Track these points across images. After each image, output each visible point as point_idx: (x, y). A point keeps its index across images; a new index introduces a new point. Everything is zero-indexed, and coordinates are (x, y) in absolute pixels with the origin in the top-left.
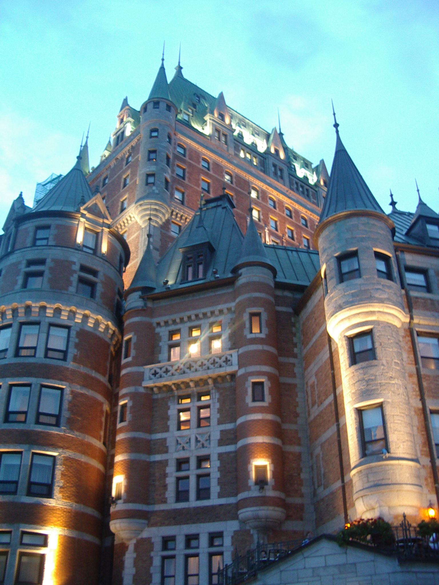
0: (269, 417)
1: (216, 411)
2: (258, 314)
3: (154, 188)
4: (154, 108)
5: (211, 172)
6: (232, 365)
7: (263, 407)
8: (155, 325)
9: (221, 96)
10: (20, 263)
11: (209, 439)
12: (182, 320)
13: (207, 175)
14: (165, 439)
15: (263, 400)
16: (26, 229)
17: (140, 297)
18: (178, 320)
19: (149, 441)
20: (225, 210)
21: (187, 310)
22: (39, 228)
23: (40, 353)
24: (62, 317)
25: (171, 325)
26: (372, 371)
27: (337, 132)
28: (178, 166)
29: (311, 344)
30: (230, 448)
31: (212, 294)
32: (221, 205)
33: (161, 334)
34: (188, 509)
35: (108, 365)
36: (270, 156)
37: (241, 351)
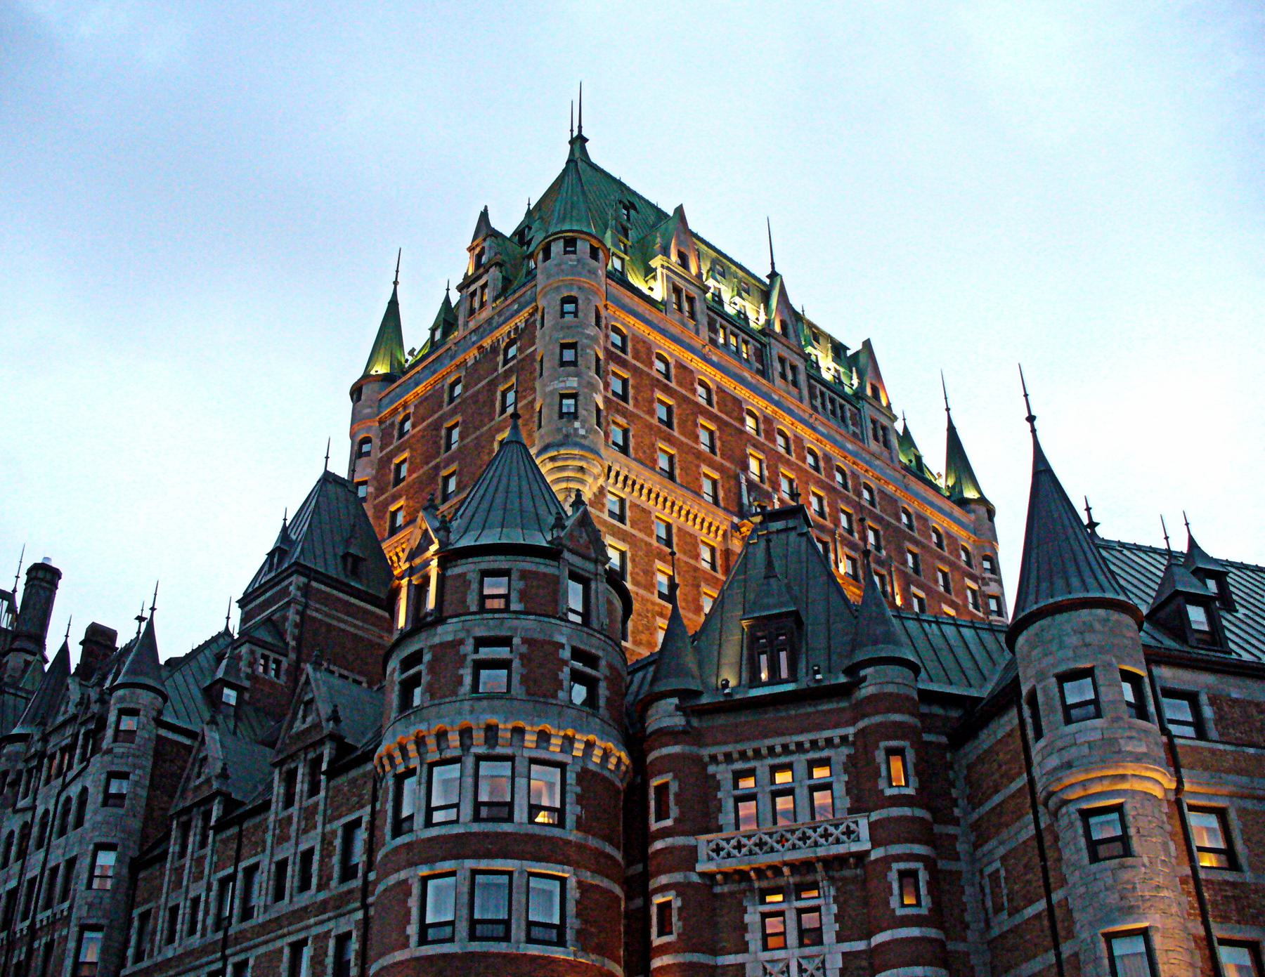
0: (932, 933)
1: (833, 917)
3: (577, 424)
4: (566, 252)
5: (673, 385)
6: (859, 840)
7: (918, 916)
8: (707, 759)
9: (680, 211)
12: (757, 752)
13: (667, 390)
16: (463, 575)
17: (678, 708)
20: (804, 539)
21: (766, 736)
22: (486, 573)
24: (552, 748)
25: (737, 761)
26: (1125, 875)
27: (1033, 431)
28: (615, 374)
29: (988, 806)
31: (810, 710)
32: (794, 528)
33: (719, 777)
36: (773, 341)
37: (875, 816)
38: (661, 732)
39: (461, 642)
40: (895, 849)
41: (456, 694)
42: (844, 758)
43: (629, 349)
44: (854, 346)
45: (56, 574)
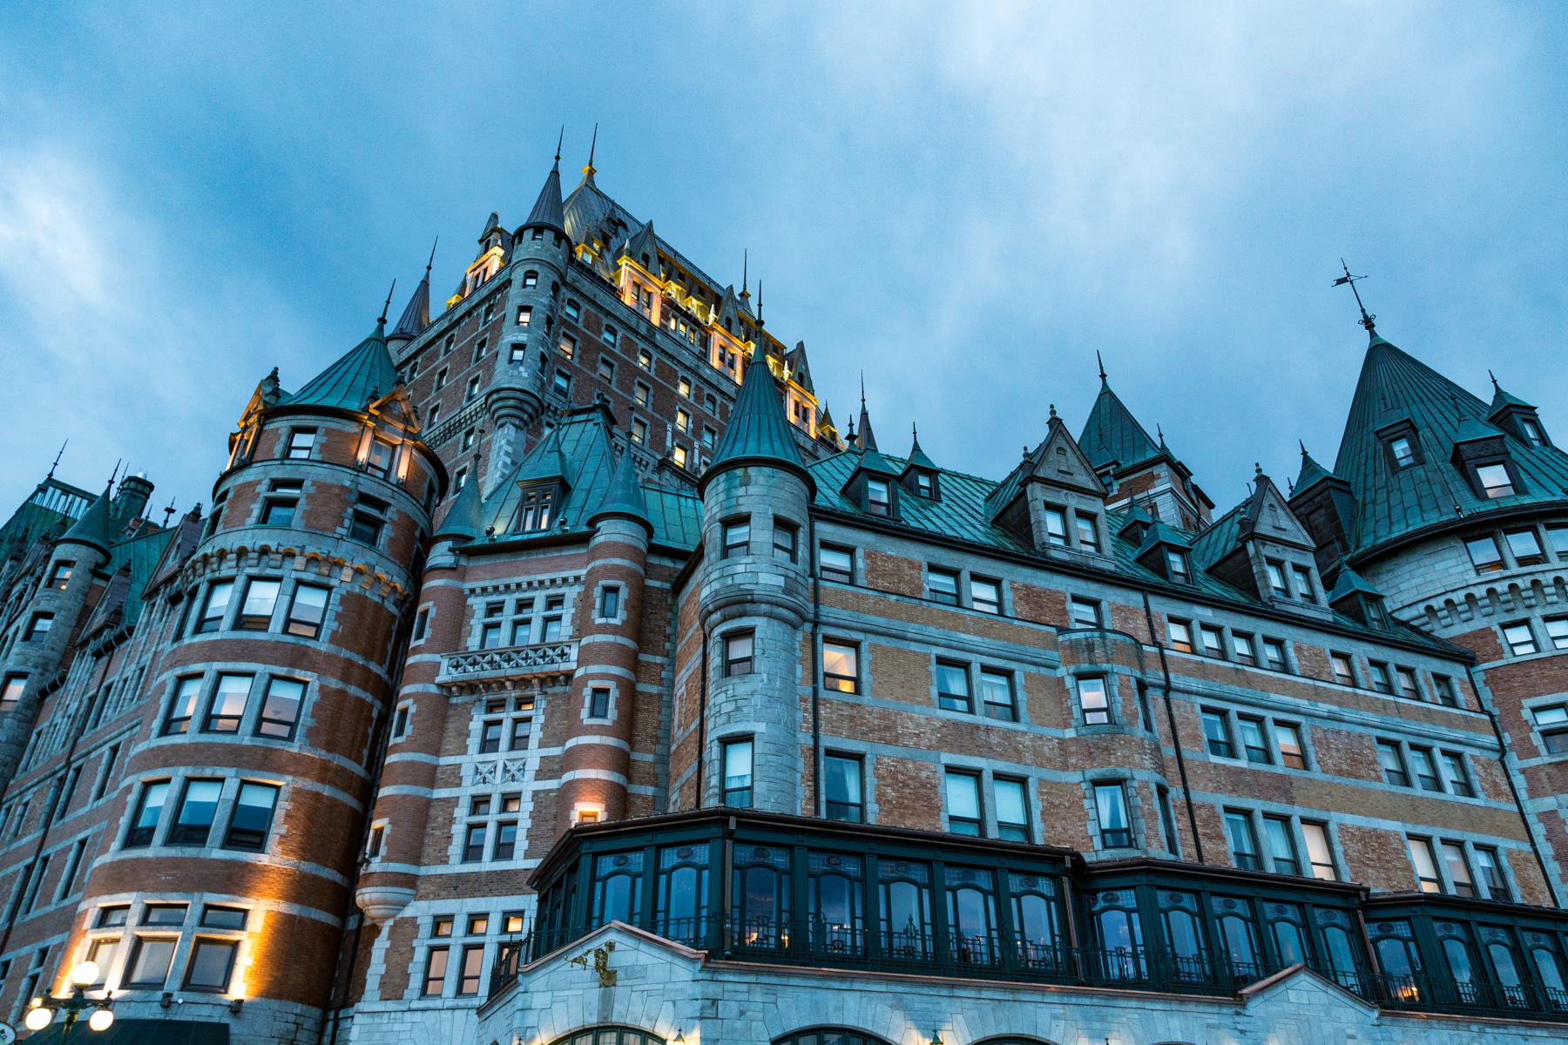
0: (610, 741)
1: (539, 726)
2: (615, 590)
8: (467, 592)
10: (259, 482)
11: (522, 769)
14: (460, 765)
15: (605, 716)
16: (278, 429)
18: (502, 588)
19: (435, 767)
20: (597, 428)
22: (297, 430)
23: (276, 626)
25: (491, 594)
30: (553, 784)
31: (558, 554)
32: (592, 420)
34: (478, 874)
35: (390, 649)
37: (584, 641)
38: (435, 569)
39: (259, 482)
40: (594, 669)
41: (243, 524)
42: (575, 595)
43: (580, 320)
44: (790, 347)
45: (151, 487)
